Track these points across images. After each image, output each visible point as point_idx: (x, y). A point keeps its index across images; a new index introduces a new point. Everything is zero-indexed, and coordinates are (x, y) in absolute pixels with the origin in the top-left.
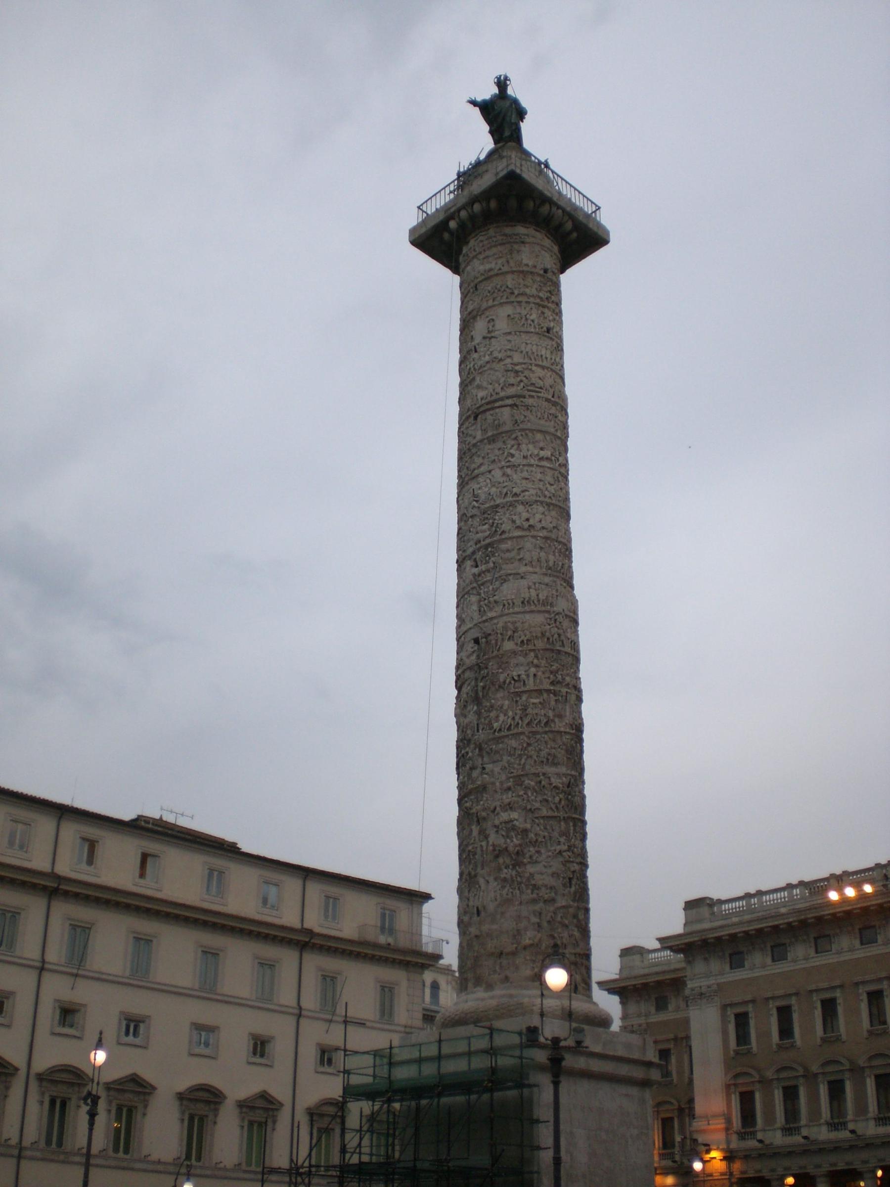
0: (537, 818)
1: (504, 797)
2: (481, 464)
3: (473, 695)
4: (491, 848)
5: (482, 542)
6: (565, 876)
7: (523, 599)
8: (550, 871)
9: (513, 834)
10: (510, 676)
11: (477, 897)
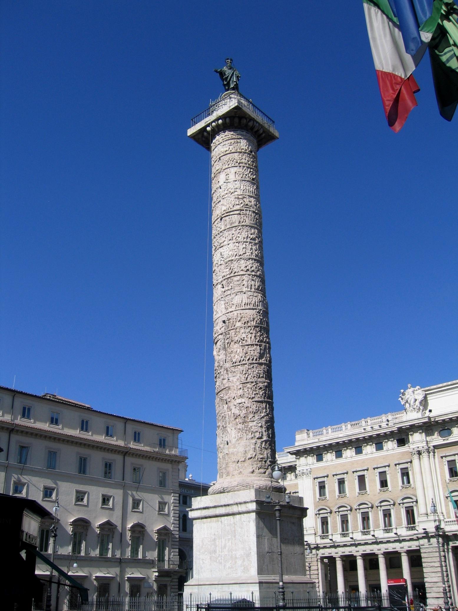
0: (253, 401)
1: (238, 392)
2: (225, 241)
3: (223, 346)
10: (240, 338)
11: (227, 437)
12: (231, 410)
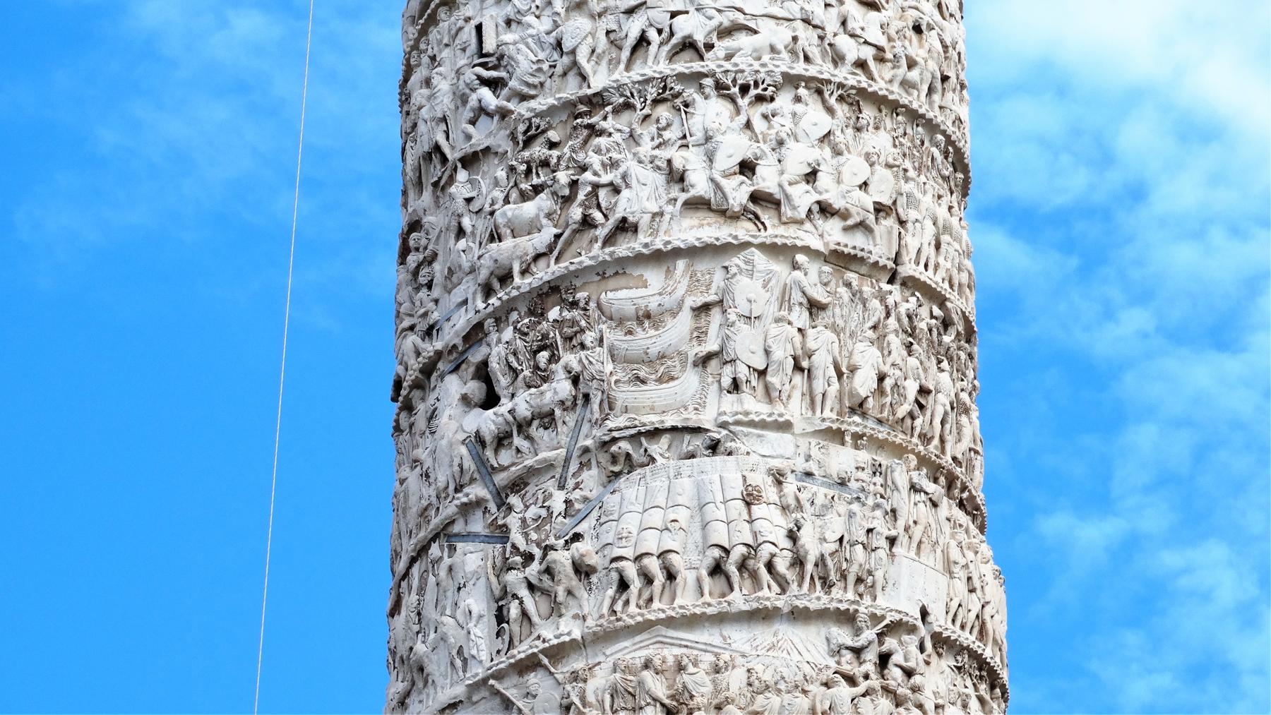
5: (517, 280)
7: (717, 553)
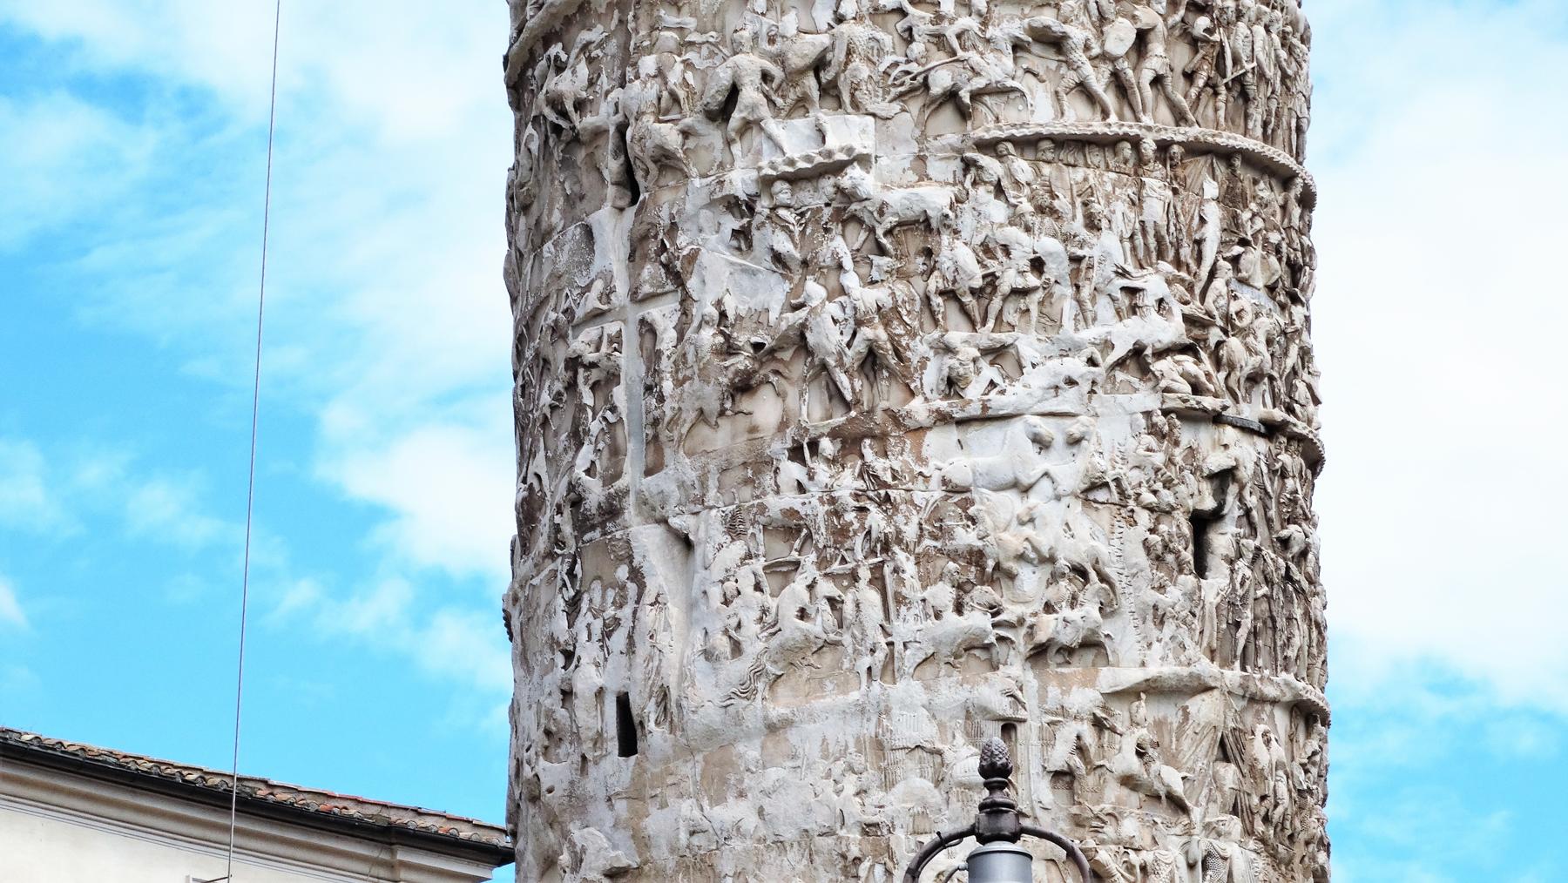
0: (988, 146)
4: (709, 337)
6: (1167, 497)
8: (1069, 471)
9: (840, 245)
12: (678, 279)
